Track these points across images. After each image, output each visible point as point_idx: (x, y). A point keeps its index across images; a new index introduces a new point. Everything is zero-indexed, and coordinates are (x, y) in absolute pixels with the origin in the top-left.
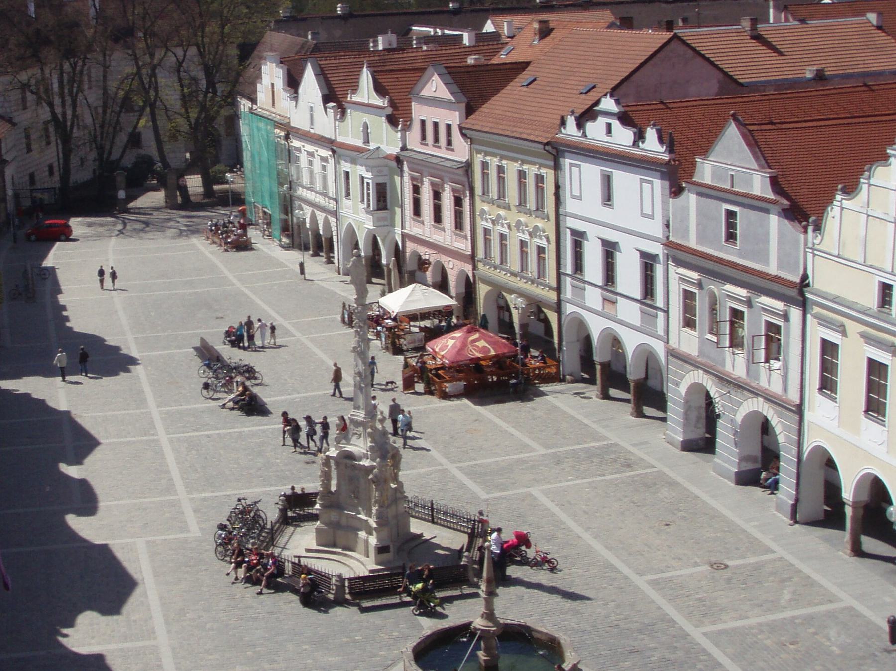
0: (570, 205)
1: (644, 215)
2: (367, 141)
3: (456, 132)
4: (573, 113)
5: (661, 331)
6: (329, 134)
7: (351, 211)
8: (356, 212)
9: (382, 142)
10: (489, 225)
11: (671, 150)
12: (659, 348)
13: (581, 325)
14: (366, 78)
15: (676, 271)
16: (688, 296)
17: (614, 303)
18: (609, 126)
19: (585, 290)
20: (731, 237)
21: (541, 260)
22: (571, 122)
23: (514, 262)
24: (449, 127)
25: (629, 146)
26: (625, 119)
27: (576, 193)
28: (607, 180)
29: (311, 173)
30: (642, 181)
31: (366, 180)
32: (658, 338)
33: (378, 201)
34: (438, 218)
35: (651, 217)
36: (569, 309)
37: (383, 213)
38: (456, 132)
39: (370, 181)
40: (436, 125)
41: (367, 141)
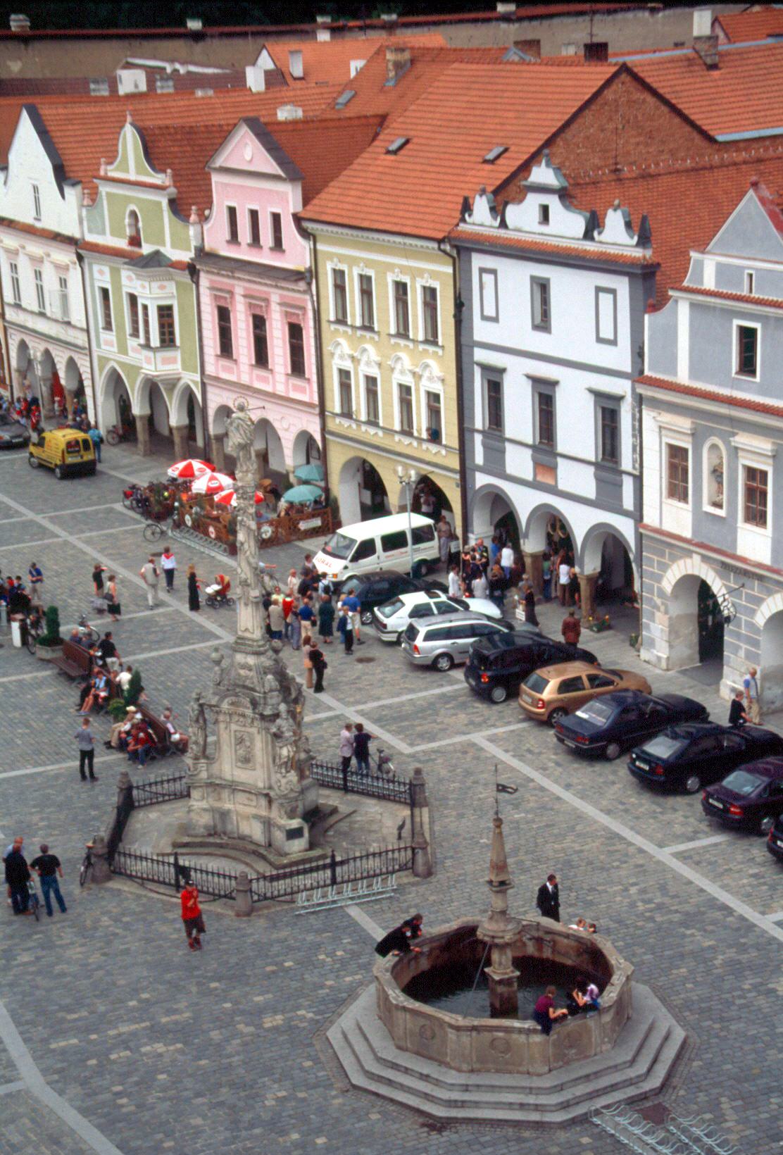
0: (481, 331)
1: (599, 340)
2: (139, 244)
3: (288, 227)
4: (483, 192)
5: (628, 502)
6: (72, 230)
7: (115, 349)
8: (123, 349)
9: (163, 244)
10: (347, 365)
11: (644, 241)
12: (626, 528)
13: (498, 500)
14: (129, 140)
15: (648, 416)
16: (677, 456)
17: (552, 469)
18: (545, 210)
19: (503, 452)
20: (747, 365)
21: (434, 412)
22: (481, 207)
23: (391, 414)
24: (276, 218)
25: (578, 239)
26: (564, 195)
27: (489, 311)
28: (542, 288)
29: (40, 289)
30: (599, 290)
31: (140, 302)
32: (626, 514)
33: (162, 334)
34: (261, 357)
35: (614, 342)
36: (481, 480)
37: (169, 354)
38: (288, 227)
39: (146, 302)
40: (254, 215)
41: (135, 241)
